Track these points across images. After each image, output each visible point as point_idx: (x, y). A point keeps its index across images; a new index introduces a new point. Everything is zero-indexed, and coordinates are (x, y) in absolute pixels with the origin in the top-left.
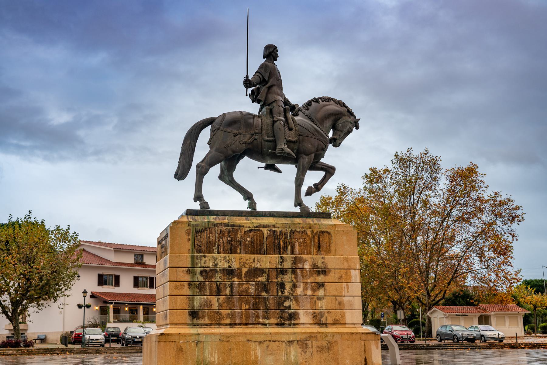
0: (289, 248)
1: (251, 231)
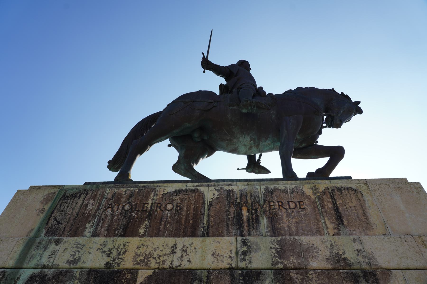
0: (264, 221)
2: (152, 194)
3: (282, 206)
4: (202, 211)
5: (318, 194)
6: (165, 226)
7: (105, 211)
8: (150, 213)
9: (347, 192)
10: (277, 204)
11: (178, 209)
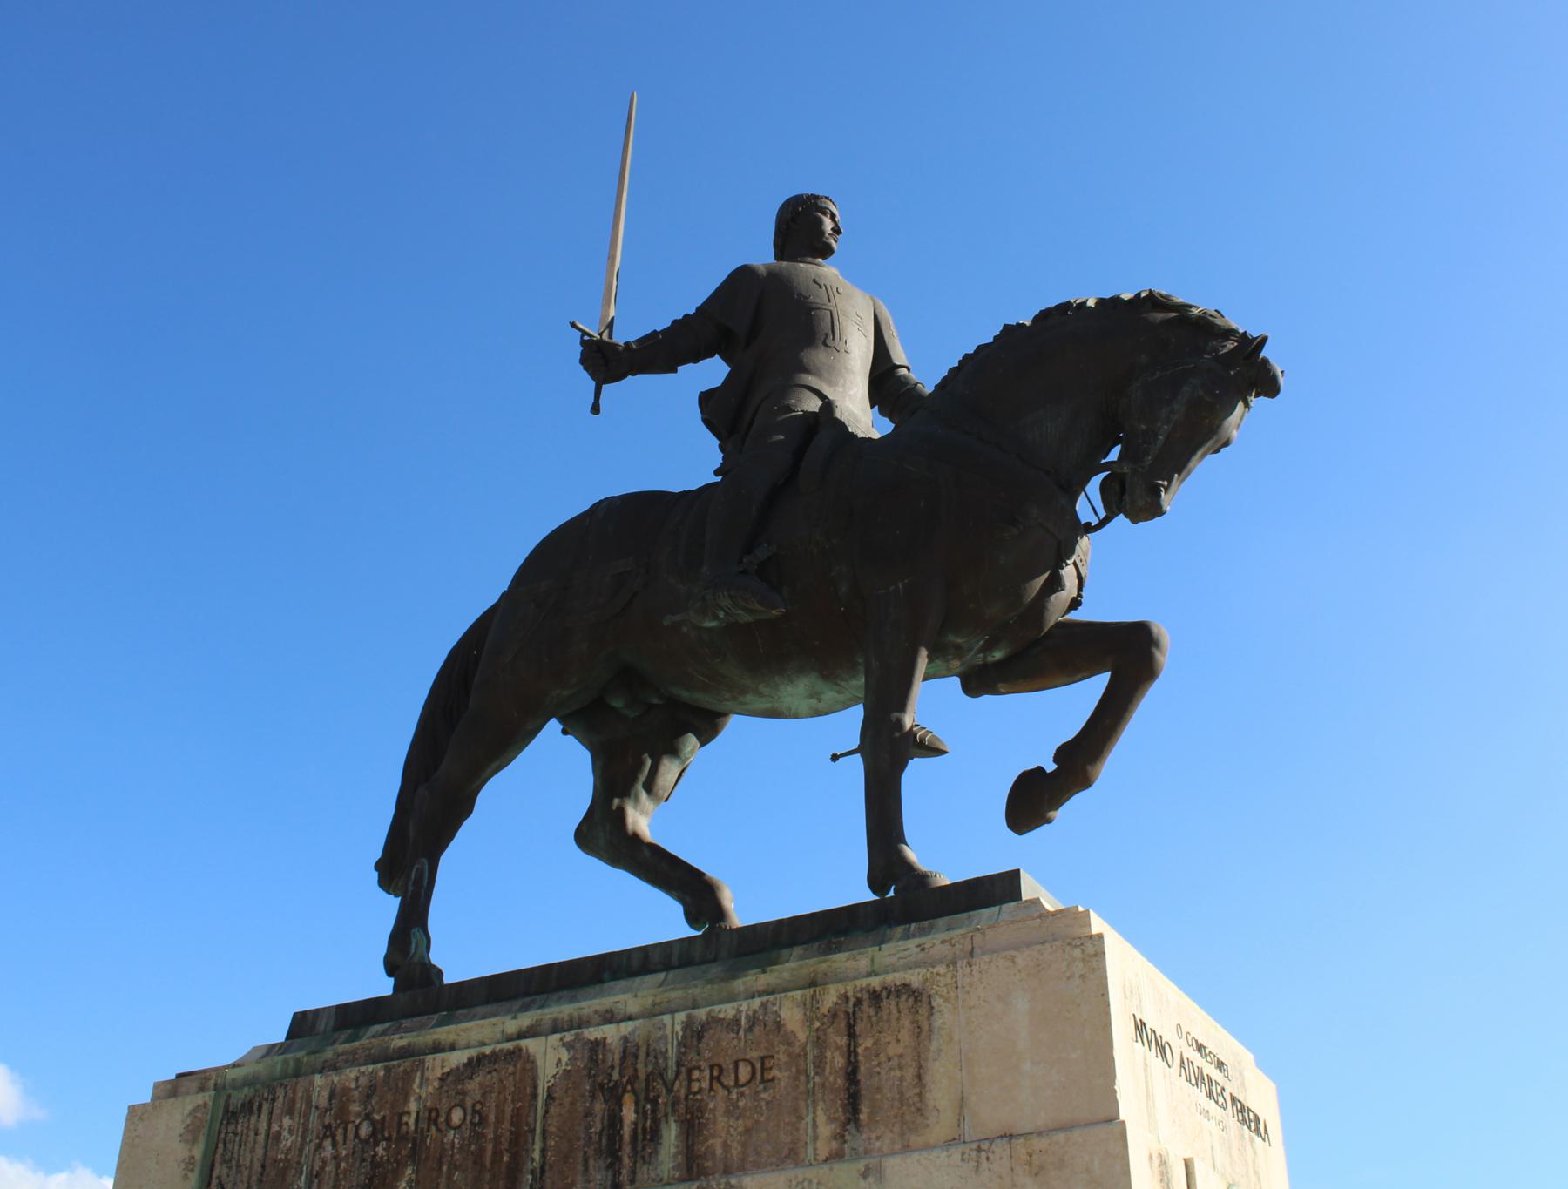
0: (671, 1134)
1: (474, 1065)
2: (417, 1080)
3: (718, 1079)
4: (531, 1120)
5: (817, 1024)
6: (450, 1177)
7: (319, 1146)
8: (414, 1144)
9: (893, 1007)
10: (707, 1073)
11: (478, 1118)
